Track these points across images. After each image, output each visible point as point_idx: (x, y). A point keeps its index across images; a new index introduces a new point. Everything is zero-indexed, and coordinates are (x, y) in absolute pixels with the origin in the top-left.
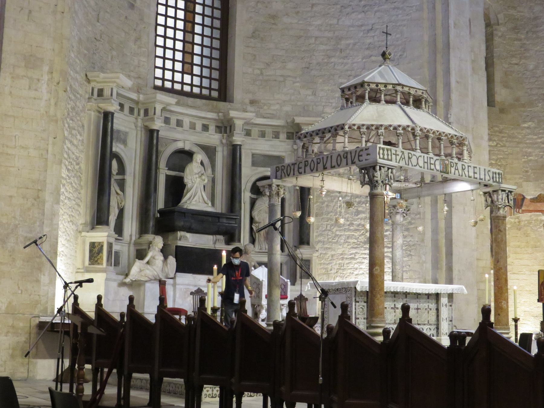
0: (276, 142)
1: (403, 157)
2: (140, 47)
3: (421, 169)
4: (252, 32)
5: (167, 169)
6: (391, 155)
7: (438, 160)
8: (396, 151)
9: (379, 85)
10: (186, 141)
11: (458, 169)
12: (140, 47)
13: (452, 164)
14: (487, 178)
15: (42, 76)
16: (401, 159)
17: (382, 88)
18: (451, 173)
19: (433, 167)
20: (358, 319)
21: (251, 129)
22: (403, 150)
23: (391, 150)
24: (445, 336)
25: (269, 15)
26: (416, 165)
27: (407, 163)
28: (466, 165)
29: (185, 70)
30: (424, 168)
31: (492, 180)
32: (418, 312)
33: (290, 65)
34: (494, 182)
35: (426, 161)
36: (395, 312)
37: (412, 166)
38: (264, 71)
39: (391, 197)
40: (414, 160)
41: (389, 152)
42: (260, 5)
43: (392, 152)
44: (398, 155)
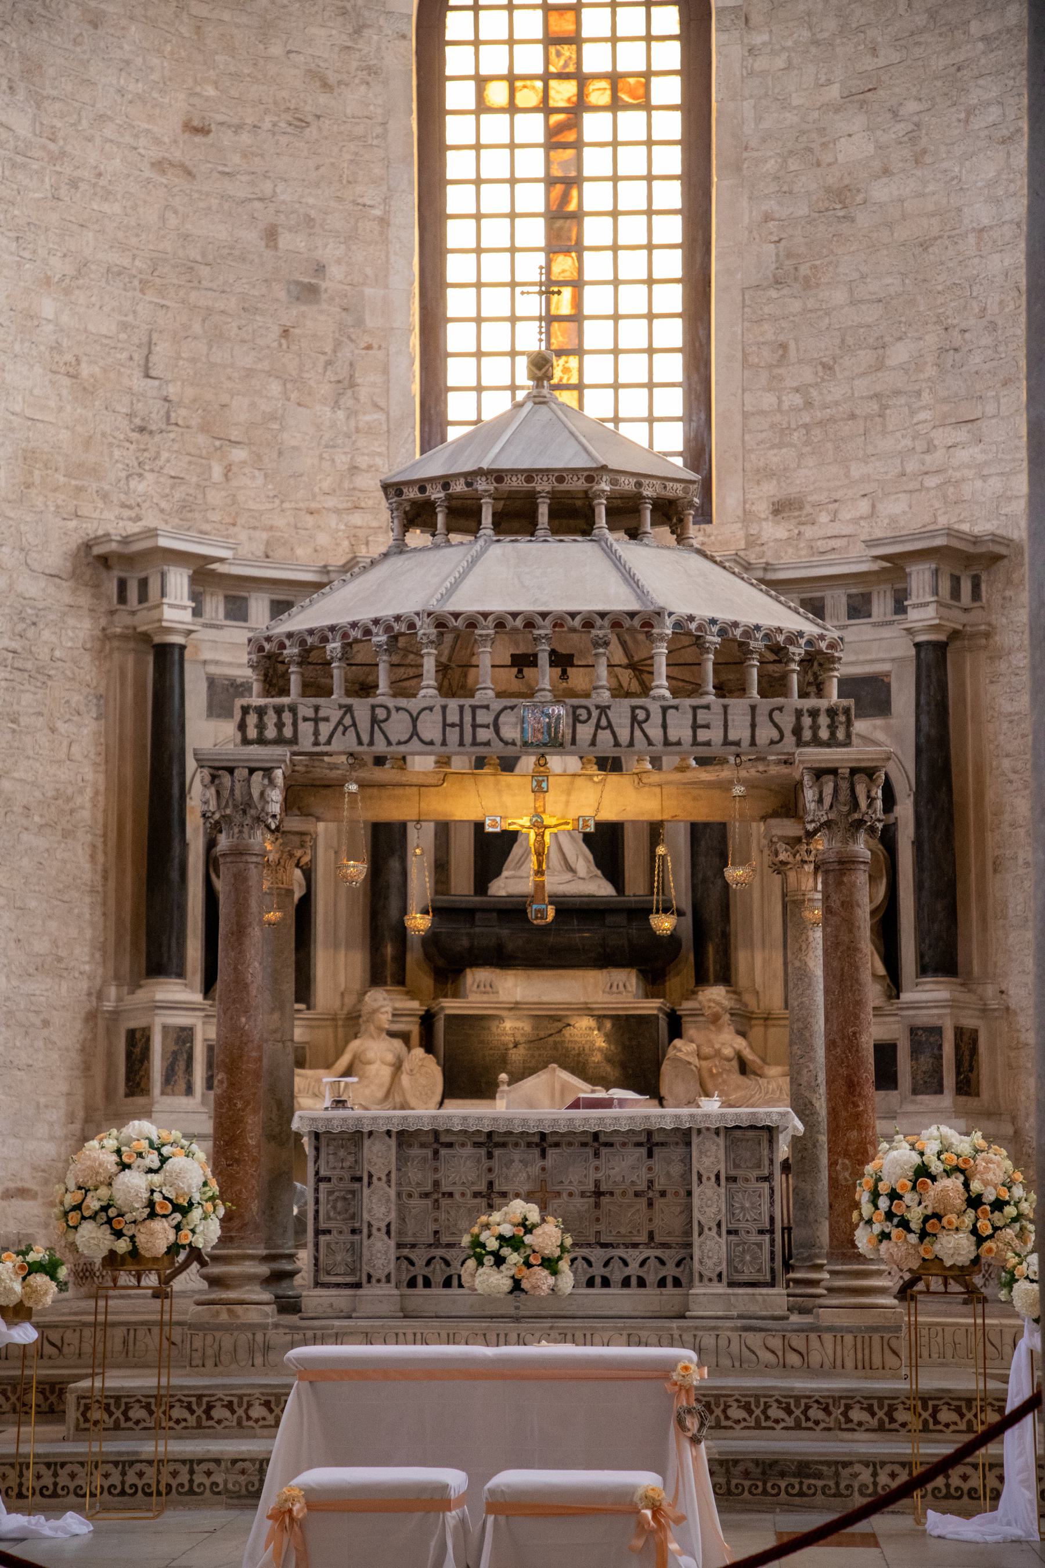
1: (347, 721)
2: (352, 413)
4: (774, 266)
6: (295, 725)
7: (512, 708)
8: (317, 709)
9: (429, 487)
11: (610, 726)
12: (352, 413)
13: (580, 711)
14: (766, 733)
16: (341, 728)
17: (436, 494)
18: (574, 742)
19: (483, 735)
22: (349, 701)
23: (293, 709)
24: (715, 1283)
25: (828, 190)
27: (365, 739)
28: (655, 708)
30: (444, 743)
31: (790, 739)
32: (597, 1205)
34: (800, 743)
35: (453, 717)
37: (389, 743)
38: (814, 393)
40: (398, 727)
41: (287, 717)
42: (793, 165)
43: (300, 715)
44: (326, 719)
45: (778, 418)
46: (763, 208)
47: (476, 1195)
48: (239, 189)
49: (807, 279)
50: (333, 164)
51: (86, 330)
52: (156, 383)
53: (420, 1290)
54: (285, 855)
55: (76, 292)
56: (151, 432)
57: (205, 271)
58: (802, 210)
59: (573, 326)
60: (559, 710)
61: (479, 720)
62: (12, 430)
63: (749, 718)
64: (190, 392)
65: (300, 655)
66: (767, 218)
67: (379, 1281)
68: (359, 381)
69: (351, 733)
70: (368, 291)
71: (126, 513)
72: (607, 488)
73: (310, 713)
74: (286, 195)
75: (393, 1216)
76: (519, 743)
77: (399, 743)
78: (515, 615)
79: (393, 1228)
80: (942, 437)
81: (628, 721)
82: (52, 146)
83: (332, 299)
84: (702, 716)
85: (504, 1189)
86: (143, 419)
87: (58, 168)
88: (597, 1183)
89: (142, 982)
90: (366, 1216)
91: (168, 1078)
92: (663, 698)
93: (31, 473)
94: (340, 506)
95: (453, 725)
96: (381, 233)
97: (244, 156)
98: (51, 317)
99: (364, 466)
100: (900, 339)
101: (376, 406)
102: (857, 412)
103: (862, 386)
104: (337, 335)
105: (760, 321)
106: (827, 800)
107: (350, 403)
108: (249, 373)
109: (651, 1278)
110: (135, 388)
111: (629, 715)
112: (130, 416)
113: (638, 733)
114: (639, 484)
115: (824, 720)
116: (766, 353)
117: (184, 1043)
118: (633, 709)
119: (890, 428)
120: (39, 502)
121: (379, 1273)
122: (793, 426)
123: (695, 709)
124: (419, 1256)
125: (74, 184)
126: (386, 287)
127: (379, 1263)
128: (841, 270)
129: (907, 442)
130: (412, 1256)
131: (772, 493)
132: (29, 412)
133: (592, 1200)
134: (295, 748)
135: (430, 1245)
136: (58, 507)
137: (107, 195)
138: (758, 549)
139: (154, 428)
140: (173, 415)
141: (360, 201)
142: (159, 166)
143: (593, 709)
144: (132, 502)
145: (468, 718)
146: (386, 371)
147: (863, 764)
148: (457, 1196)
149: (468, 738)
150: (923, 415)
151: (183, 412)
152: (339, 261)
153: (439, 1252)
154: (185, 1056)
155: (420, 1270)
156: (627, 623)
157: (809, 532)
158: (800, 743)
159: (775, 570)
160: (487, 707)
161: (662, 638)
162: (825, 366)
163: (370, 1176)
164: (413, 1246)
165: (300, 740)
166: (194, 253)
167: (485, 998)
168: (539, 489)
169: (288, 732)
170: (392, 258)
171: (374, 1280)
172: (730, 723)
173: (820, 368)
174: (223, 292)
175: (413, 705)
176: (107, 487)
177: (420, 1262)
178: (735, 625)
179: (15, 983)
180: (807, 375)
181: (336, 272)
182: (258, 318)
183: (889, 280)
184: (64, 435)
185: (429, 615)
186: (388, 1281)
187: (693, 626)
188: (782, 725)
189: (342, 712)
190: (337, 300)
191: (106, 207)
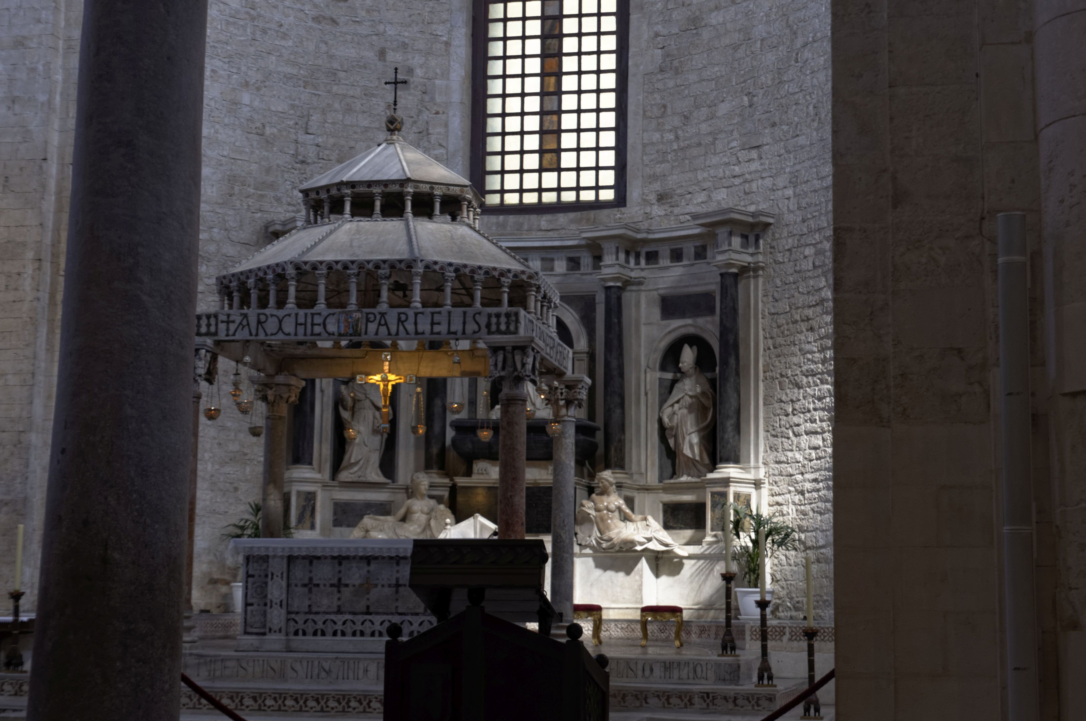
1: (245, 322)
3: (287, 337)
4: (660, 61)
6: (217, 325)
7: (333, 314)
11: (386, 324)
15: (24, 267)
16: (241, 327)
17: (324, 196)
18: (366, 333)
19: (317, 329)
20: (252, 604)
26: (275, 331)
27: (254, 332)
30: (296, 334)
32: (397, 592)
35: (301, 320)
36: (339, 592)
37: (266, 335)
38: (680, 133)
39: (394, 383)
41: (213, 321)
44: (233, 322)
45: (661, 147)
46: (655, 29)
47: (332, 585)
48: (363, 30)
49: (677, 69)
50: (419, 14)
51: (269, 110)
52: (312, 136)
53: (301, 637)
54: (278, 397)
55: (264, 89)
56: (308, 164)
57: (342, 75)
58: (675, 30)
59: (555, 98)
60: (358, 315)
61: (315, 322)
62: (221, 165)
63: (462, 319)
64: (332, 141)
65: (237, 286)
66: (657, 35)
67: (275, 632)
68: (431, 131)
69: (246, 328)
70: (437, 82)
71: (291, 208)
72: (412, 190)
73: (225, 318)
74: (391, 31)
75: (284, 596)
76: (336, 333)
77: (272, 334)
78: (337, 262)
79: (284, 603)
80: (743, 155)
81: (395, 321)
82: (252, 12)
83: (416, 87)
84: (437, 318)
85: (347, 582)
86: (304, 157)
87: (256, 23)
88: (397, 579)
89: (290, 467)
90: (269, 596)
91: (300, 519)
92: (416, 308)
93: (233, 188)
95: (301, 324)
96: (446, 50)
97: (368, 11)
98: (248, 103)
100: (723, 101)
101: (440, 145)
102: (703, 142)
103: (704, 128)
104: (419, 107)
105: (652, 93)
106: (500, 365)
107: (426, 144)
108: (367, 129)
109: (349, 631)
110: (300, 140)
111: (397, 317)
112: (295, 155)
113: (401, 328)
114: (432, 188)
115: (503, 320)
117: (310, 500)
118: (399, 314)
119: (718, 151)
120: (238, 203)
121: (276, 628)
123: (433, 314)
124: (300, 618)
125: (264, 31)
126: (448, 79)
127: (275, 621)
128: (694, 63)
130: (297, 618)
132: (233, 155)
133: (394, 589)
134: (216, 338)
135: (306, 613)
136: (249, 206)
137: (285, 36)
138: (649, 221)
139: (310, 161)
140: (321, 154)
141: (434, 33)
142: (316, 19)
143: (377, 314)
144: (295, 202)
145: (309, 320)
146: (446, 125)
147: (519, 344)
148: (322, 586)
149: (309, 331)
150: (734, 144)
151: (327, 152)
152: (421, 66)
153: (311, 617)
154: (310, 508)
155: (301, 626)
156: (398, 266)
157: (676, 211)
158: (490, 333)
159: (654, 233)
160: (319, 314)
161: (417, 274)
163: (272, 574)
164: (297, 613)
165: (219, 333)
166: (336, 65)
167: (481, 477)
168: (374, 191)
169: (213, 329)
170: (452, 63)
171: (272, 631)
172: (451, 321)
173: (683, 118)
174: (353, 85)
175: (281, 313)
176: (279, 195)
177: (301, 622)
178: (465, 266)
179: (217, 467)
180: (676, 121)
181: (419, 72)
182: (373, 99)
184: (254, 167)
185: (291, 263)
186: (280, 630)
187: (437, 267)
188: (480, 322)
189: (241, 318)
190: (420, 87)
191: (283, 43)
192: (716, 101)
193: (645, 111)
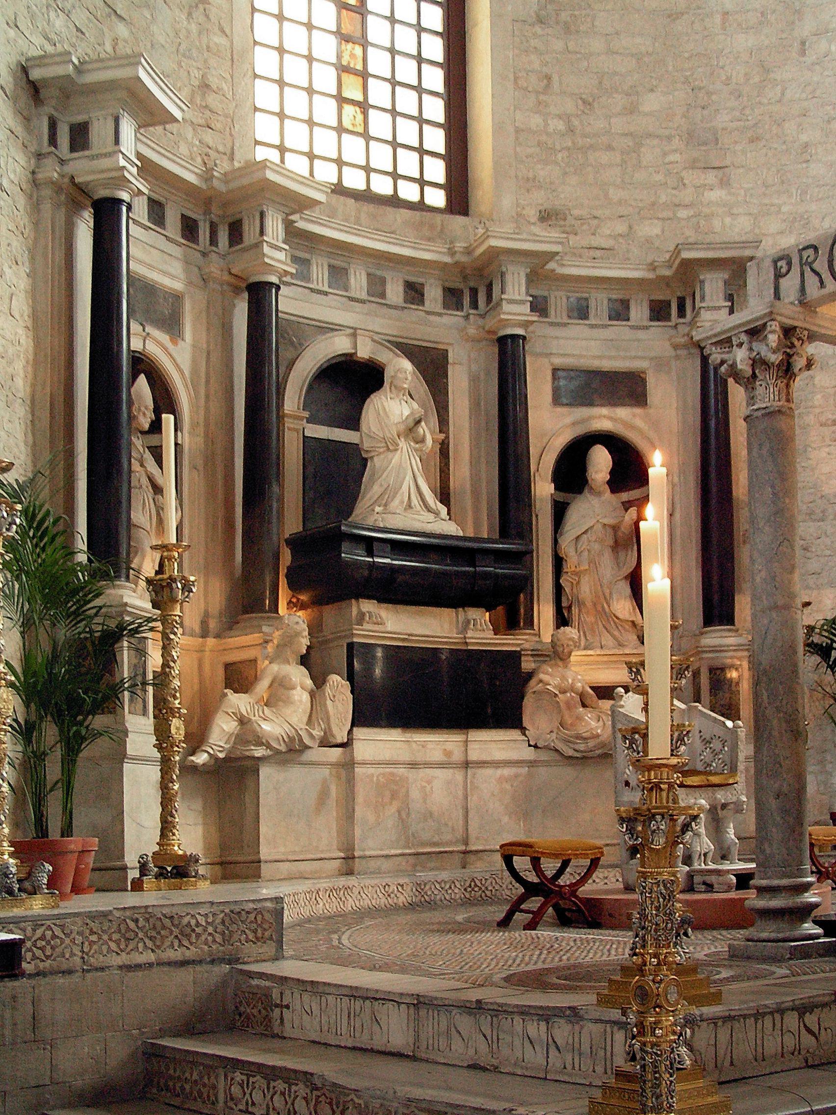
0: (619, 330)
5: (306, 414)
10: (359, 332)
21: (546, 294)
29: (347, 123)
33: (652, 103)
38: (576, 122)
45: (544, 138)
94: (194, 120)
99: (214, 87)
100: (652, 90)
102: (614, 144)
107: (202, 19)
116: (533, 78)
119: (645, 163)
122: (558, 147)
129: (659, 177)
131: (540, 202)
150: (672, 158)
162: (584, 102)
167: (376, 628)
173: (580, 102)
180: (569, 106)
183: (638, 40)
192: (639, 89)
193: (516, 79)
